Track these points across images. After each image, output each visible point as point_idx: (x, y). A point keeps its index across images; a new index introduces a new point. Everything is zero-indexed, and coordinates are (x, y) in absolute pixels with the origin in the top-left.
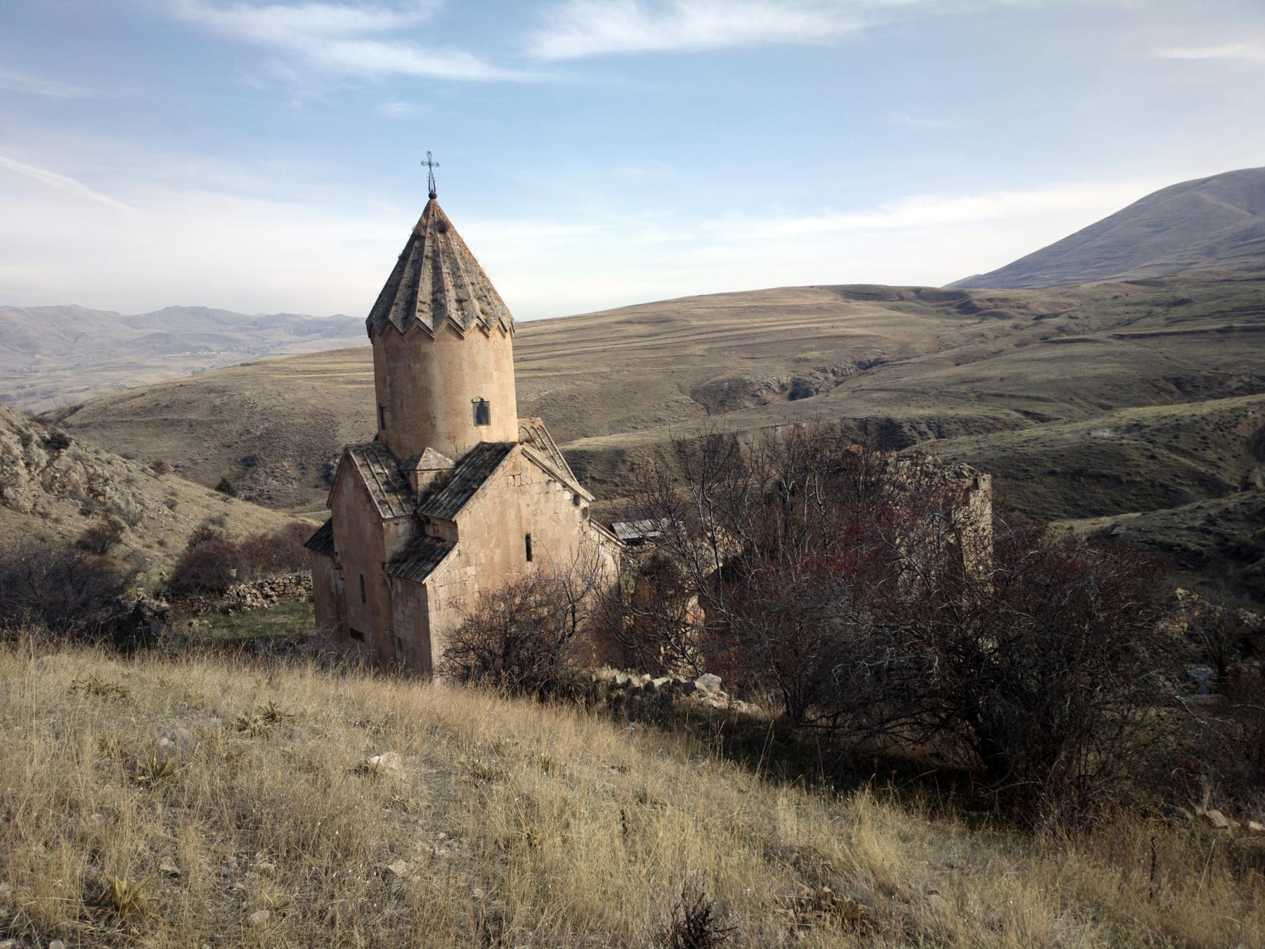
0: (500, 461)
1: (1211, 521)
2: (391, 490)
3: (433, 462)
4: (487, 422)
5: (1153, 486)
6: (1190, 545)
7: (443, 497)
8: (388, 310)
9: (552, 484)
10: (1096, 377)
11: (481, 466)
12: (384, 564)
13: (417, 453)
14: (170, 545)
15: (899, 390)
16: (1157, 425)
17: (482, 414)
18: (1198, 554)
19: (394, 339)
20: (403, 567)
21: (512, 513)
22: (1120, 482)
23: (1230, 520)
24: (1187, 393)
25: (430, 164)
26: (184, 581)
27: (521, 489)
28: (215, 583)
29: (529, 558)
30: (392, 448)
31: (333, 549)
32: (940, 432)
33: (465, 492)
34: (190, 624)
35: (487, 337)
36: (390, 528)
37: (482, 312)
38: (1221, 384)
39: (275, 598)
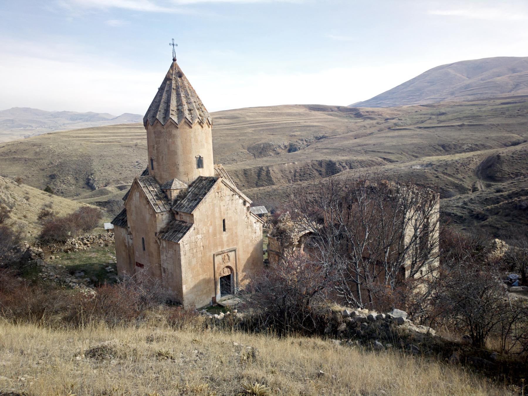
0: (212, 186)
1: (465, 203)
2: (159, 199)
3: (178, 186)
4: (202, 167)
6: (458, 213)
7: (185, 202)
8: (156, 113)
9: (234, 196)
10: (412, 144)
11: (202, 188)
12: (156, 233)
13: (170, 181)
14: (29, 217)
15: (334, 149)
16: (438, 164)
17: (200, 163)
18: (461, 217)
19: (159, 128)
20: (166, 235)
21: (217, 209)
23: (473, 203)
24: (447, 151)
25: (173, 45)
26: (46, 238)
27: (221, 198)
28: (60, 239)
29: (224, 230)
30: (158, 179)
31: (127, 225)
32: (350, 166)
33: (196, 200)
34: (51, 258)
35: (202, 127)
36: (159, 217)
37: (200, 115)
38: (460, 147)
39: (89, 245)
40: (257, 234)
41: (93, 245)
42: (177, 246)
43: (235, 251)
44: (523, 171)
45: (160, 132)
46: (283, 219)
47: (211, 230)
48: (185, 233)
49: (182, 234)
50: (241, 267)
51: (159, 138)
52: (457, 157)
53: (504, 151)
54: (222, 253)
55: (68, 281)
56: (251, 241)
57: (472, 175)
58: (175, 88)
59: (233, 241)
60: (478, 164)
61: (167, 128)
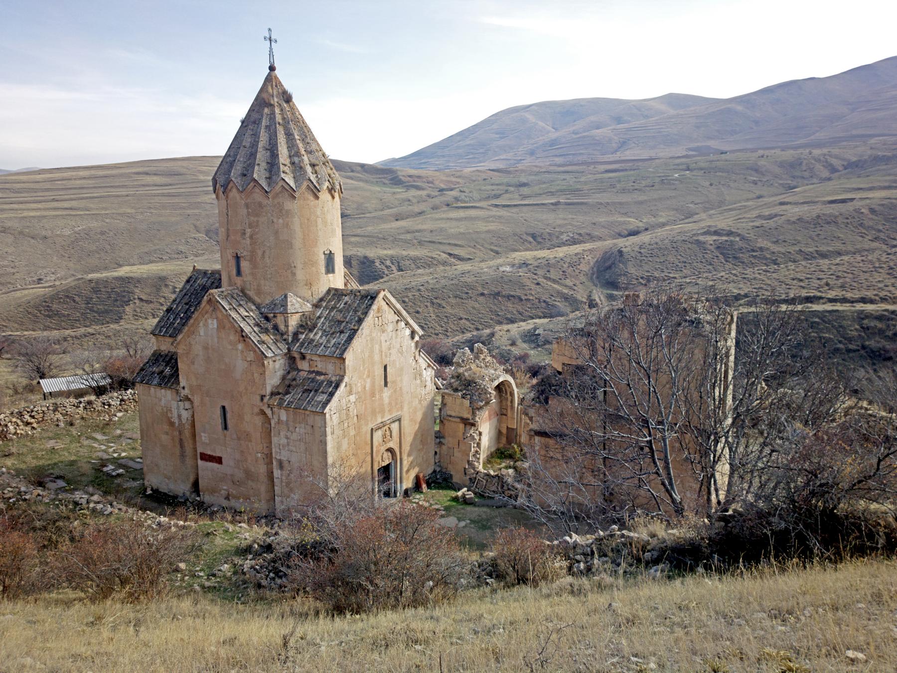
2: (266, 331)
3: (298, 306)
5: (540, 302)
7: (317, 336)
10: (488, 232)
12: (262, 397)
13: (278, 297)
15: (368, 236)
16: (536, 264)
20: (288, 398)
22: (521, 300)
24: (539, 243)
29: (386, 384)
30: (251, 293)
31: (177, 382)
32: (399, 266)
35: (333, 197)
38: (558, 237)
40: (427, 387)
41: (42, 425)
42: (318, 418)
43: (399, 420)
44: (656, 274)
45: (260, 205)
46: (463, 361)
47: (368, 386)
48: (332, 395)
49: (325, 396)
50: (406, 448)
51: (257, 215)
52: (561, 252)
53: (627, 244)
54: (383, 424)
55: (84, 501)
56: (420, 401)
57: (584, 280)
58: (281, 121)
59: (396, 404)
60: (592, 264)
61: (274, 198)
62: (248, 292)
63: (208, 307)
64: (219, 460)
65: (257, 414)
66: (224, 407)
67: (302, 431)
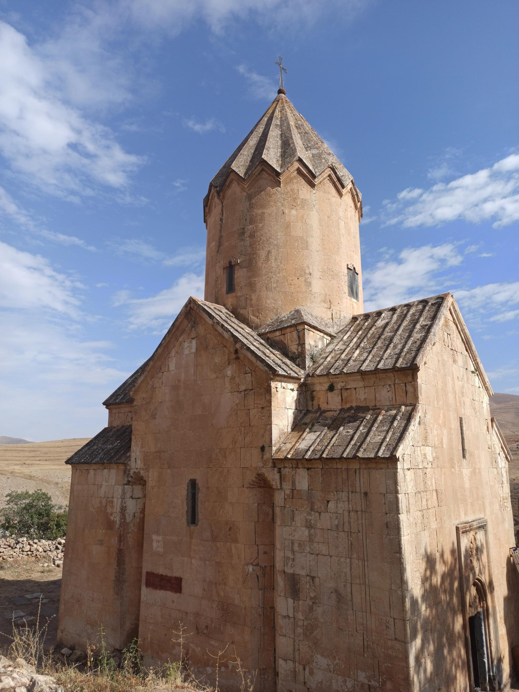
62: (242, 311)
63: (186, 322)
64: (175, 585)
65: (253, 486)
66: (193, 484)
67: (343, 506)
